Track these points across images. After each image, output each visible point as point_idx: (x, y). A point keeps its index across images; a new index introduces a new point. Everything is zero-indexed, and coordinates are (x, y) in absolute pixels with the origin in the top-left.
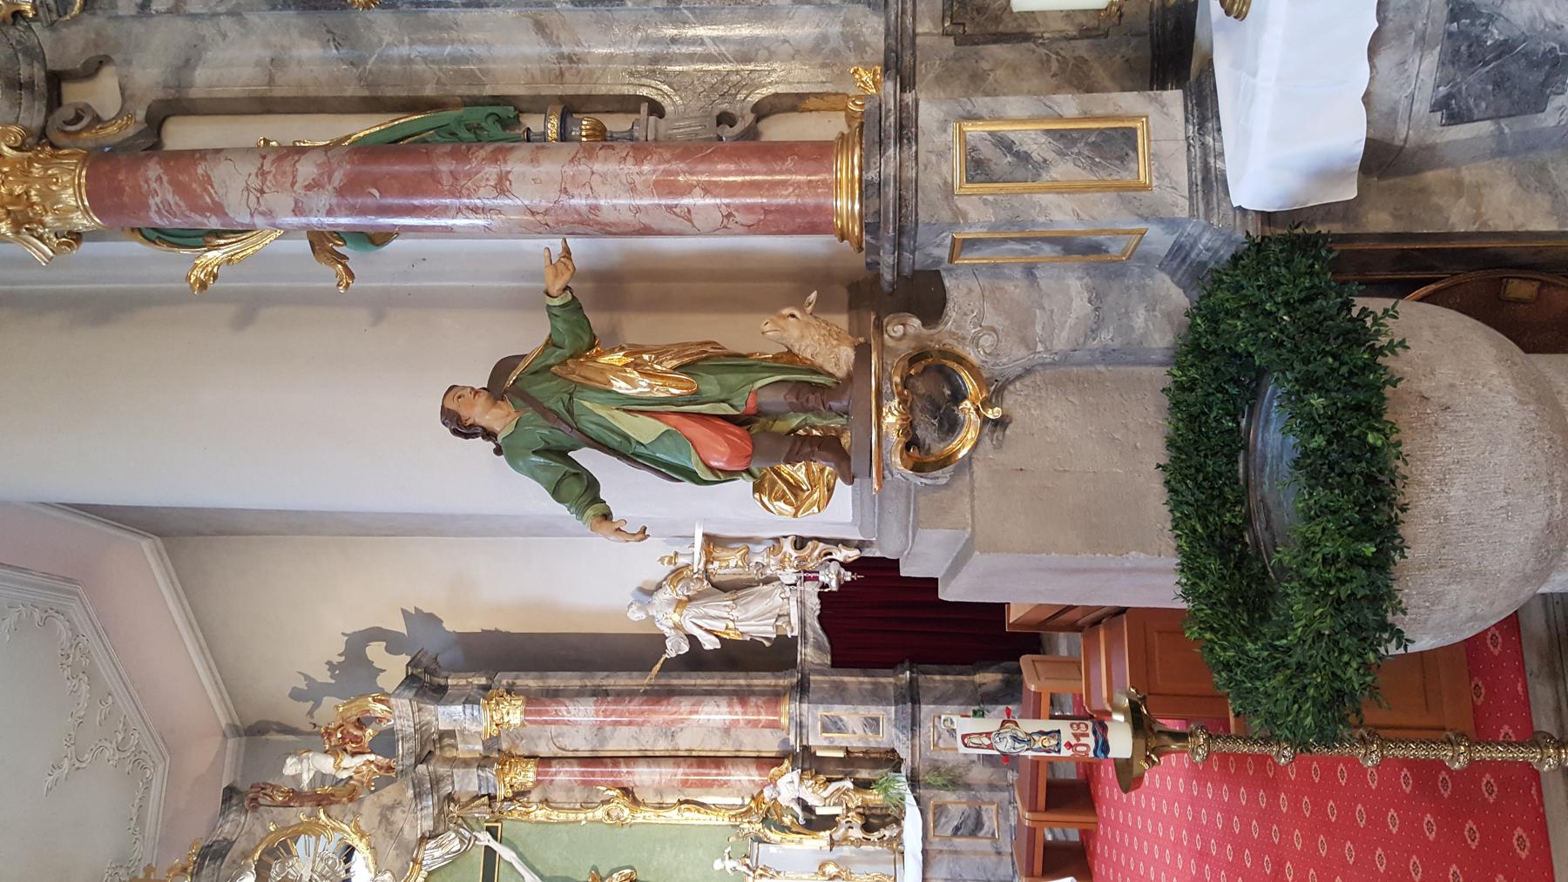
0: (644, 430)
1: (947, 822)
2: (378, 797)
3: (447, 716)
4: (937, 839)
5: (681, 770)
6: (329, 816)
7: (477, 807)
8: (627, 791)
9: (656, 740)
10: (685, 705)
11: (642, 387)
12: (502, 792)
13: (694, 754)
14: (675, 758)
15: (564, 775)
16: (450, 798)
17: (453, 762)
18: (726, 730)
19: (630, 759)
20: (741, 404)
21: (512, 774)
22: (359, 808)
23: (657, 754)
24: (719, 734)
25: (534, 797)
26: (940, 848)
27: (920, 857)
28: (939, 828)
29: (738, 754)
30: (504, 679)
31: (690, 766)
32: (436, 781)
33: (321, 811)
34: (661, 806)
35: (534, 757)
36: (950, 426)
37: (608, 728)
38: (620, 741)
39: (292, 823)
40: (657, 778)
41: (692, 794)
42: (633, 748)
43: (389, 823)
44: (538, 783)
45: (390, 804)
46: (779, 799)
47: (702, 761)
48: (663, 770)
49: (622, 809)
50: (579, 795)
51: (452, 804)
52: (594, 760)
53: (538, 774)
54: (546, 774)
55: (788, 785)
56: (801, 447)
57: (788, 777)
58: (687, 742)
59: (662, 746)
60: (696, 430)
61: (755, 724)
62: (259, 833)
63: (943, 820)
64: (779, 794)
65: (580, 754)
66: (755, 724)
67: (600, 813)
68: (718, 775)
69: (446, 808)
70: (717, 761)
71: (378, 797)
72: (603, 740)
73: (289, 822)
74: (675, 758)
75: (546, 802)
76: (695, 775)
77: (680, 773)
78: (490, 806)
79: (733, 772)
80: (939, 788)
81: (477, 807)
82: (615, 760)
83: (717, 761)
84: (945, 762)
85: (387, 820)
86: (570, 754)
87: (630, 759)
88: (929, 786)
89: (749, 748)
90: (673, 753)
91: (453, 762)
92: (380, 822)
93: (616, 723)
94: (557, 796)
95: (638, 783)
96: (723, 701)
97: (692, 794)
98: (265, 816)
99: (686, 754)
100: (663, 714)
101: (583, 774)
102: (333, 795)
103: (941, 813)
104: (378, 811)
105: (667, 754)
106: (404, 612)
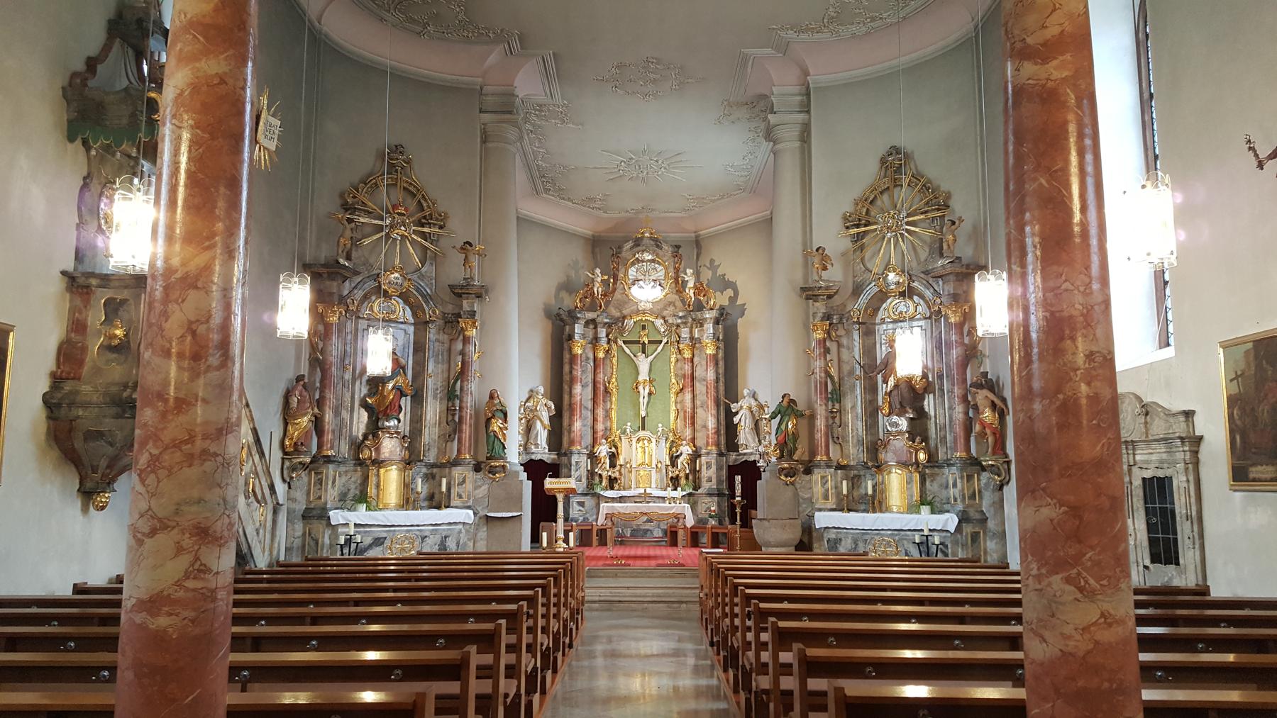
0: (783, 427)
3: (709, 327)
8: (681, 390)
10: (714, 412)
11: (790, 427)
12: (681, 346)
15: (687, 367)
17: (691, 328)
18: (705, 427)
19: (693, 391)
20: (788, 442)
25: (679, 356)
30: (721, 346)
32: (685, 323)
34: (676, 403)
36: (786, 476)
37: (705, 383)
38: (699, 387)
41: (681, 414)
42: (697, 392)
44: (685, 358)
47: (693, 418)
49: (675, 389)
50: (680, 372)
52: (692, 378)
56: (782, 452)
58: (699, 411)
59: (698, 403)
60: (783, 434)
61: (708, 437)
66: (708, 437)
67: (674, 381)
70: (693, 424)
72: (700, 381)
74: (694, 408)
75: (677, 360)
77: (689, 410)
82: (693, 386)
83: (693, 424)
87: (693, 391)
89: (698, 435)
91: (691, 328)
93: (707, 387)
94: (679, 364)
96: (715, 426)
97: (681, 414)
100: (711, 404)
106: (745, 304)
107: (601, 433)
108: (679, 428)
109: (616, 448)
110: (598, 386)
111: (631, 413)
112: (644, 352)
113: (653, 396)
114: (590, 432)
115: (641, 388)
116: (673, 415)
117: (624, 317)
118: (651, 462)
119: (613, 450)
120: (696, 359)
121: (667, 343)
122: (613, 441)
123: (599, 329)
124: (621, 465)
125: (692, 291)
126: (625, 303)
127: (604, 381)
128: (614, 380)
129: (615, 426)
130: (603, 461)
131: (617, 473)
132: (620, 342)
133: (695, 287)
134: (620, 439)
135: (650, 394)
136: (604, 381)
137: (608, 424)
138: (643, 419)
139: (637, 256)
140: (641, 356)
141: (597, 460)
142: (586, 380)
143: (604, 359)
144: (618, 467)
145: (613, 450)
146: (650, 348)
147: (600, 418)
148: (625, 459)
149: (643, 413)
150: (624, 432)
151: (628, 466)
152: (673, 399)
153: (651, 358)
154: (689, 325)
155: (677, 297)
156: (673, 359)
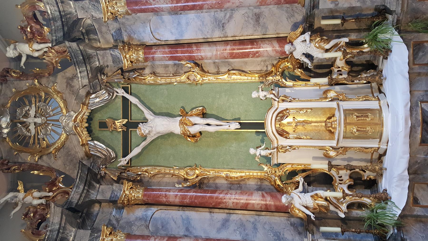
1: (423, 55)
2: (65, 73)
4: (417, 66)
5: (229, 47)
6: (40, 84)
7: (115, 75)
8: (197, 65)
9: (213, 31)
13: (237, 38)
14: (226, 42)
16: (101, 70)
21: (130, 53)
22: (56, 80)
23: (215, 40)
24: (252, 23)
26: (419, 71)
27: (407, 75)
28: (417, 59)
29: (264, 36)
31: (234, 45)
33: (36, 81)
35: (143, 45)
39: (24, 89)
40: (215, 53)
43: (72, 87)
44: (146, 59)
45: (71, 76)
46: (294, 53)
48: (218, 47)
51: (102, 76)
53: (145, 53)
54: (149, 53)
55: (301, 43)
57: (302, 38)
62: (9, 94)
63: (421, 54)
64: (295, 49)
65: (169, 43)
68: (252, 48)
69: (100, 77)
71: (65, 73)
73: (22, 88)
74: (226, 42)
76: (238, 49)
78: (122, 75)
79: (262, 45)
80: (418, 32)
81: (115, 75)
84: (424, 13)
85: (70, 85)
86: (163, 43)
87: (198, 44)
88: (407, 32)
90: (224, 39)
92: (67, 86)
95: (204, 57)
98: (11, 85)
99: (231, 39)
101: (171, 53)
102: (41, 73)
103: (419, 49)
104: (65, 80)
105: (220, 40)
107: (269, 198)
108: (259, 68)
109: (293, 174)
110: (187, 201)
111: (234, 146)
112: (135, 125)
113: (208, 111)
114: (266, 218)
115: (193, 130)
116: (236, 78)
117: (88, 156)
118: (323, 110)
119: (300, 179)
120: (149, 40)
121: (126, 90)
122: (280, 178)
123: (99, 197)
124: (331, 166)
125: (36, 46)
126: (68, 154)
127: (180, 190)
128: (182, 173)
129: (256, 173)
130: (324, 203)
131: (342, 172)
132: (123, 161)
133: (29, 41)
134: (279, 165)
135: (204, 115)
136: (180, 190)
137: (252, 183)
138: (243, 126)
139: (5, 136)
140: (143, 129)
141: (320, 212)
142: (180, 222)
143: (146, 190)
144: (333, 172)
145: (300, 179)
146: (135, 116)
147: (243, 199)
148: (315, 158)
149: (234, 126)
150: (267, 159)
151: (332, 153)
152: (212, 78)
153: (148, 114)
154: (90, 51)
155: (60, 76)
156: (150, 79)
